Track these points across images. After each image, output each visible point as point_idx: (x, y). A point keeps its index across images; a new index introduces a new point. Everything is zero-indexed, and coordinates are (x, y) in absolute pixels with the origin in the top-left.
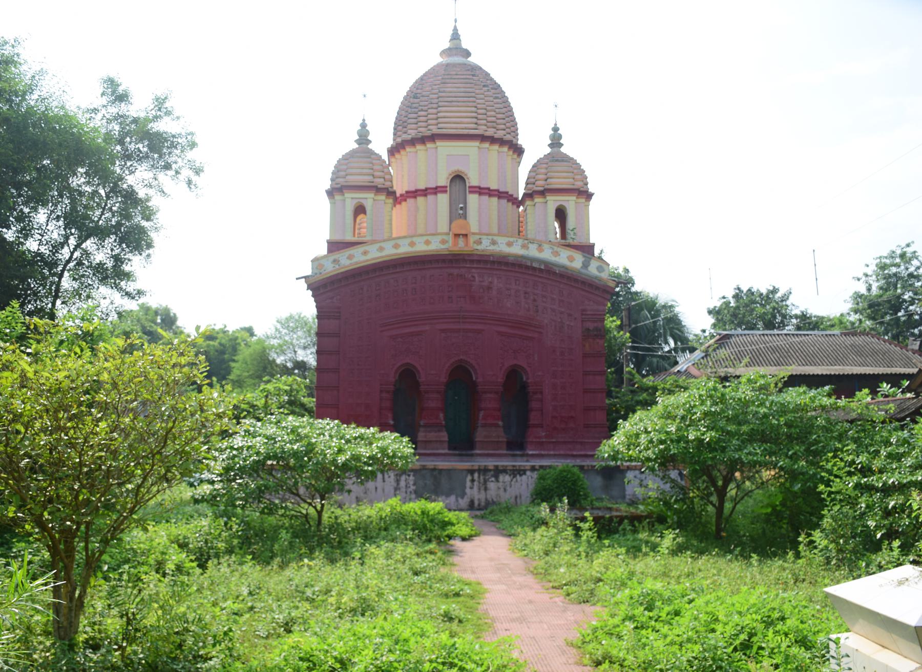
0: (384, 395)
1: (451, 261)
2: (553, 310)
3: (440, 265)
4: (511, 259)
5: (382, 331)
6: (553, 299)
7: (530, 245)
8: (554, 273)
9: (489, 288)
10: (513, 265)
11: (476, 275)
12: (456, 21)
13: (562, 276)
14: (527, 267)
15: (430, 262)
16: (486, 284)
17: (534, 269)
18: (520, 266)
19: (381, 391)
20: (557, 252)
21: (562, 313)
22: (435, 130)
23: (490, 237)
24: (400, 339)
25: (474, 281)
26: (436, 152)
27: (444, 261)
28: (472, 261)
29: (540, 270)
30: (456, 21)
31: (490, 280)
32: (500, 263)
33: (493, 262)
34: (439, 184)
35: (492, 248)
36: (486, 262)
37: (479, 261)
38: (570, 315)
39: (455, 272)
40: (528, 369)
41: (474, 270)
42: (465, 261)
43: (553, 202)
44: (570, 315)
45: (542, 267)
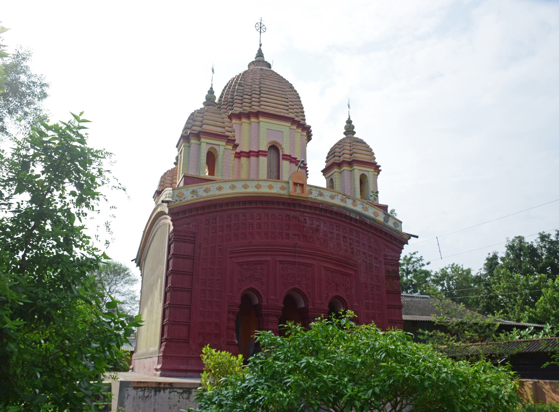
0: (231, 316)
1: (289, 204)
2: (364, 253)
3: (281, 207)
4: (335, 209)
5: (231, 258)
6: (364, 244)
7: (347, 200)
8: (366, 224)
9: (317, 230)
10: (336, 213)
11: (307, 219)
12: (261, 45)
13: (371, 226)
14: (346, 217)
15: (273, 203)
16: (314, 226)
17: (351, 218)
18: (341, 215)
19: (229, 312)
20: (366, 208)
21: (370, 256)
23: (318, 190)
24: (245, 266)
25: (306, 223)
26: (259, 126)
27: (284, 204)
28: (305, 207)
29: (356, 220)
30: (261, 45)
31: (317, 223)
32: (326, 211)
33: (321, 209)
34: (261, 149)
35: (320, 198)
36: (316, 208)
37: (310, 207)
38: (376, 258)
39: (292, 213)
40: (347, 301)
41: (306, 215)
42: (300, 205)
43: (358, 170)
44: (376, 258)
45: (358, 218)
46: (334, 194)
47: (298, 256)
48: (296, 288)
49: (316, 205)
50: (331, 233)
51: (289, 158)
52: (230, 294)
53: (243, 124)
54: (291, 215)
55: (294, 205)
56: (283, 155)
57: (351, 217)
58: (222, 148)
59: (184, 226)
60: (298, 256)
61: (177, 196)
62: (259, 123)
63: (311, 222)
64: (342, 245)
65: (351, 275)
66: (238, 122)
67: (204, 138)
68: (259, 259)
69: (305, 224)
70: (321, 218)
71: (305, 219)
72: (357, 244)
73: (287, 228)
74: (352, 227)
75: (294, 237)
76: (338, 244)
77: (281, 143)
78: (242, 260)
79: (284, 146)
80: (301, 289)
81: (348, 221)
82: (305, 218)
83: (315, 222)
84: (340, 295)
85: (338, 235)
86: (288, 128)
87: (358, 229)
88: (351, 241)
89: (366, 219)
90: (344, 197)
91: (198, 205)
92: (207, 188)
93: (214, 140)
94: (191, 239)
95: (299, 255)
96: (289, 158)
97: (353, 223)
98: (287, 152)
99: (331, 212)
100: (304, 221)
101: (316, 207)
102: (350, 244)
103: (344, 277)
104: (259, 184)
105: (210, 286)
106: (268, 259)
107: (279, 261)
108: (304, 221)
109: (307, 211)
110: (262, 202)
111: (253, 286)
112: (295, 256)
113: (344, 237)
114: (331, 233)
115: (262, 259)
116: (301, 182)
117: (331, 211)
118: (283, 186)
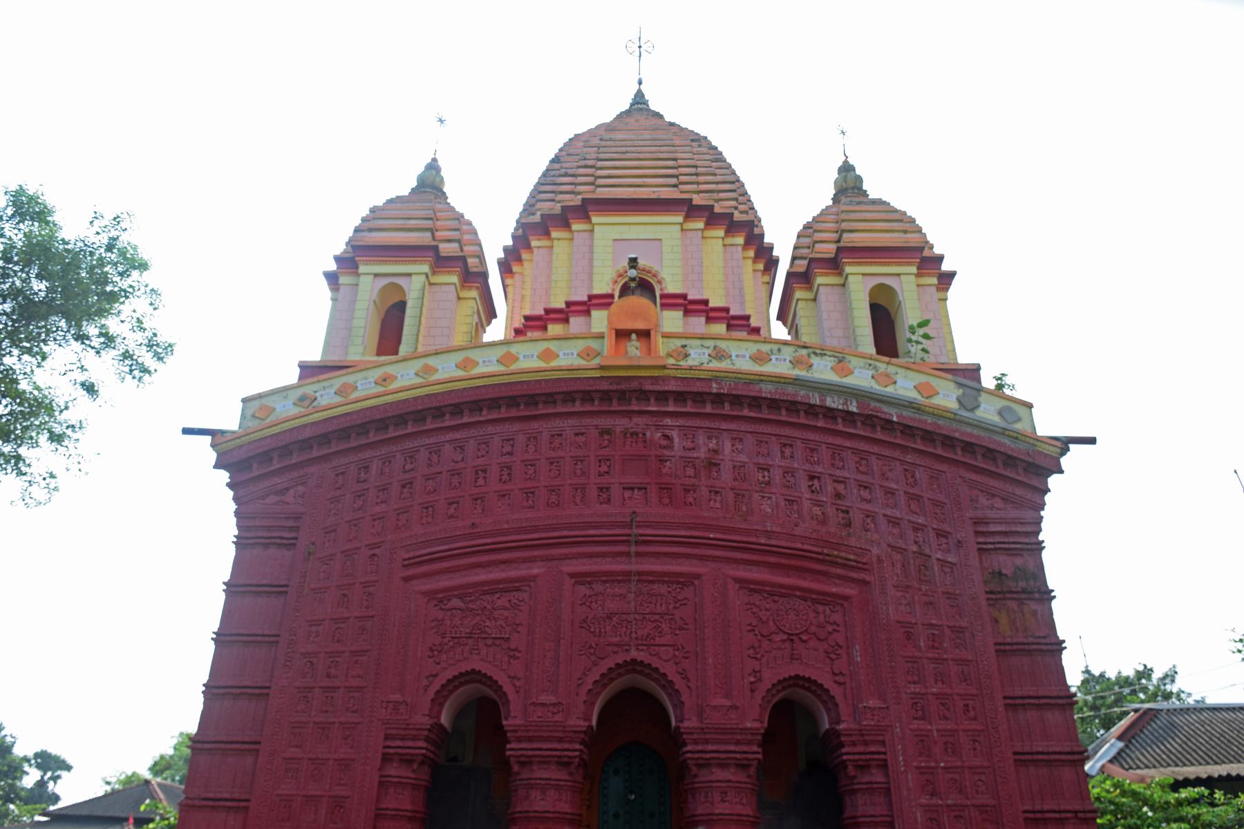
0: (393, 770)
1: (606, 396)
2: (894, 522)
3: (578, 407)
4: (767, 390)
5: (407, 579)
6: (890, 492)
7: (815, 360)
8: (888, 424)
9: (712, 464)
10: (774, 404)
11: (675, 434)
12: (640, 83)
13: (907, 430)
14: (812, 410)
15: (550, 398)
16: (702, 453)
17: (830, 413)
18: (793, 406)
19: (386, 759)
20: (887, 375)
21: (917, 528)
22: (587, 192)
23: (711, 343)
24: (456, 602)
25: (670, 447)
26: (592, 239)
27: (587, 396)
28: (662, 396)
29: (848, 416)
30: (640, 83)
31: (712, 445)
32: (736, 400)
33: (718, 399)
34: (596, 291)
35: (715, 364)
36: (700, 397)
37: (680, 397)
38: (941, 534)
39: (620, 424)
40: (836, 691)
41: (668, 421)
42: (643, 395)
43: (860, 281)
44: (941, 534)
45: (853, 408)
46: (766, 348)
47: (638, 554)
48: (634, 661)
49: (698, 388)
50: (764, 468)
51: (681, 301)
52: (397, 697)
53: (556, 242)
54: (618, 429)
55: (623, 396)
56: (662, 296)
57: (830, 409)
58: (417, 282)
59: (268, 501)
60: (638, 554)
61: (253, 416)
62: (592, 231)
63: (689, 444)
64: (806, 504)
65: (846, 598)
66: (545, 243)
67: (367, 263)
68: (503, 575)
69: (666, 452)
70: (724, 426)
71: (667, 437)
72: (865, 494)
73: (604, 468)
74: (838, 441)
75: (627, 494)
76: (791, 502)
77: (655, 268)
78: (444, 582)
79: (665, 274)
80: (656, 663)
81: (820, 424)
82: (667, 432)
83: (701, 439)
84: (807, 673)
85: (789, 472)
86: (678, 227)
87: (863, 446)
88: (841, 487)
89: (885, 408)
90: (804, 352)
91: (307, 434)
92: (345, 385)
93: (396, 262)
94: (285, 535)
95: (642, 549)
96: (681, 301)
97: (840, 427)
98: (673, 287)
99: (756, 402)
100: (664, 443)
101: (701, 394)
102: (838, 496)
103: (820, 608)
104: (509, 353)
105: (328, 676)
106: (535, 571)
107: (572, 575)
108: (664, 443)
109: (671, 408)
110: (513, 401)
111: (477, 666)
112: (628, 554)
113: (812, 478)
114: (764, 468)
115: (513, 574)
116: (640, 325)
117: (755, 398)
118: (589, 348)
